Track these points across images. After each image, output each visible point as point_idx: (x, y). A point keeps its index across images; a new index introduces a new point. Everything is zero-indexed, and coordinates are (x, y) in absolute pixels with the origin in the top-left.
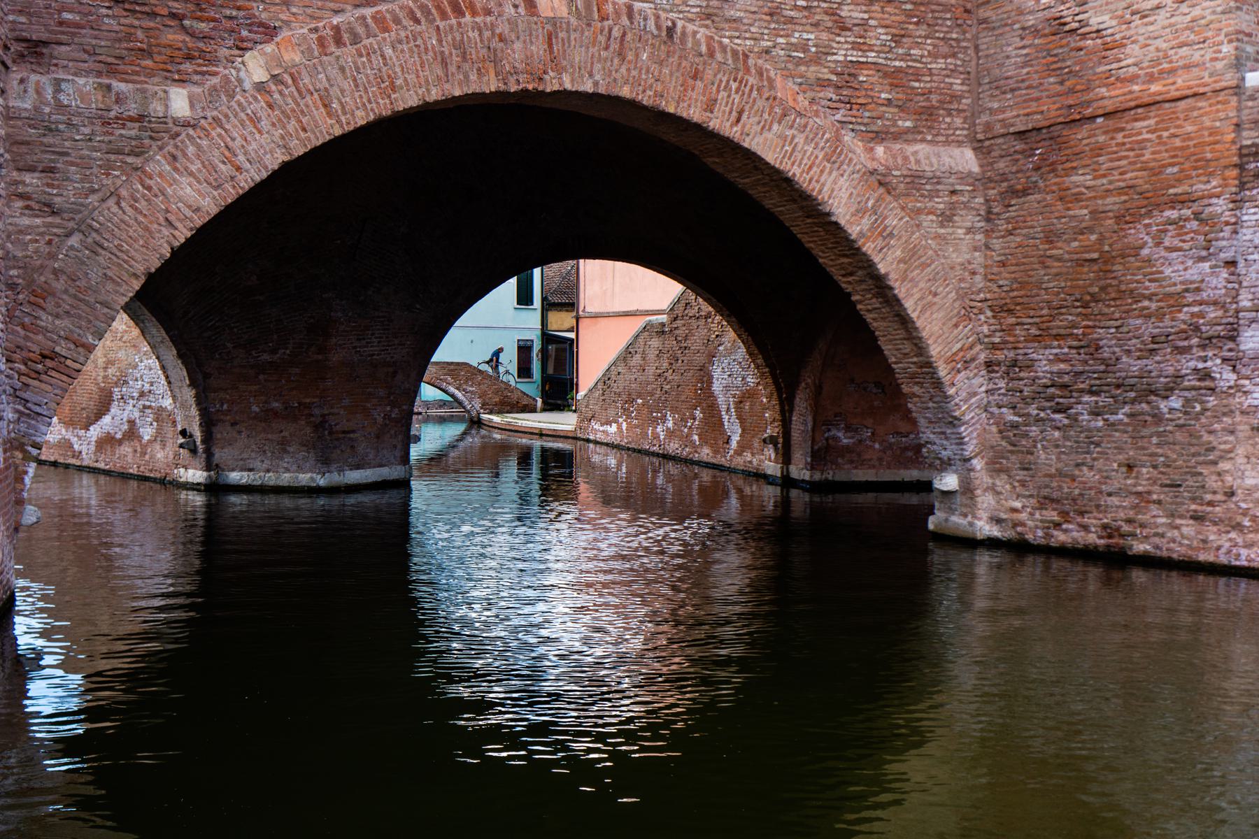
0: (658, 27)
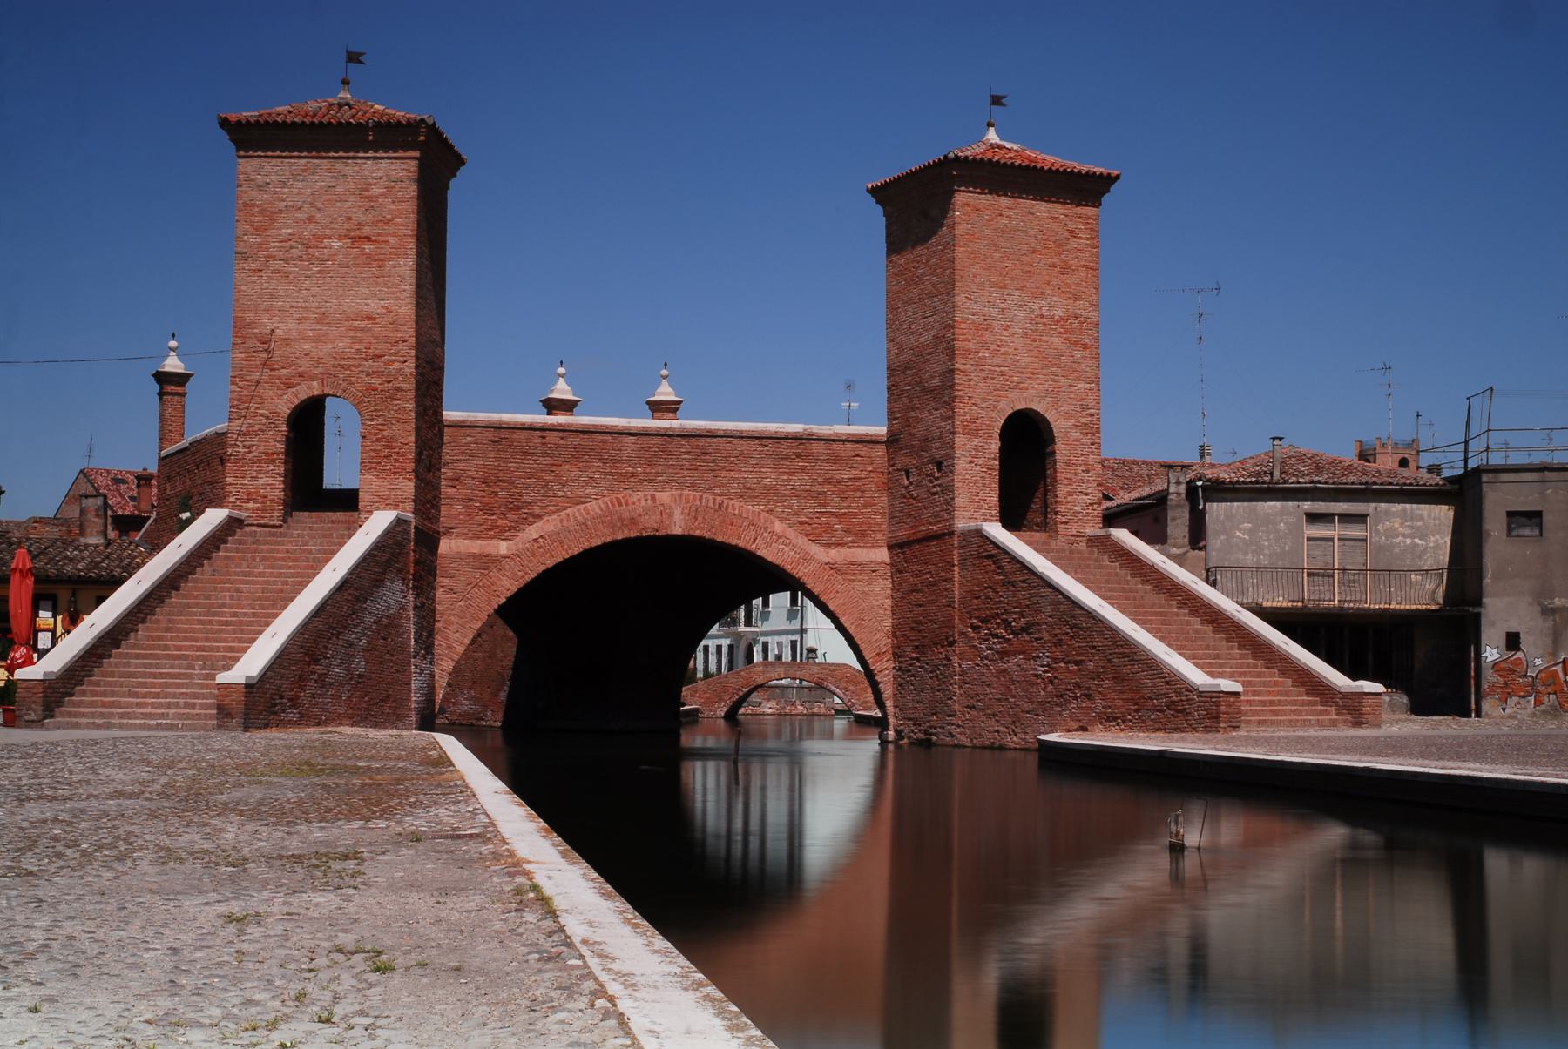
0: (714, 503)
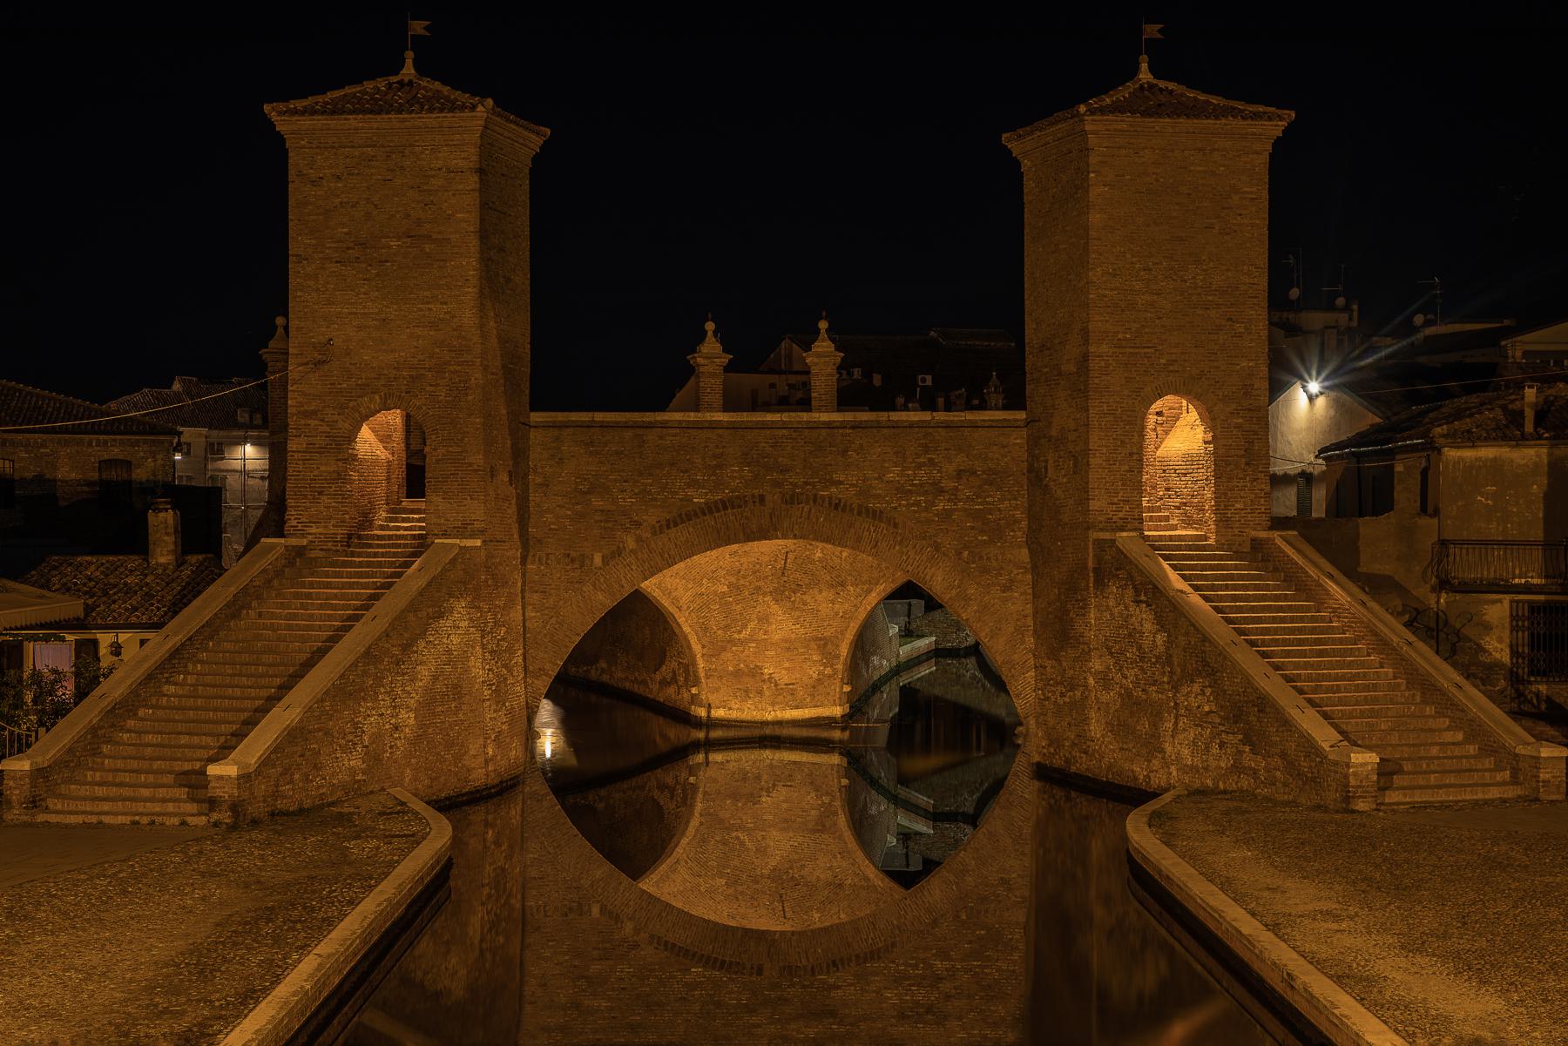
0: (830, 504)
